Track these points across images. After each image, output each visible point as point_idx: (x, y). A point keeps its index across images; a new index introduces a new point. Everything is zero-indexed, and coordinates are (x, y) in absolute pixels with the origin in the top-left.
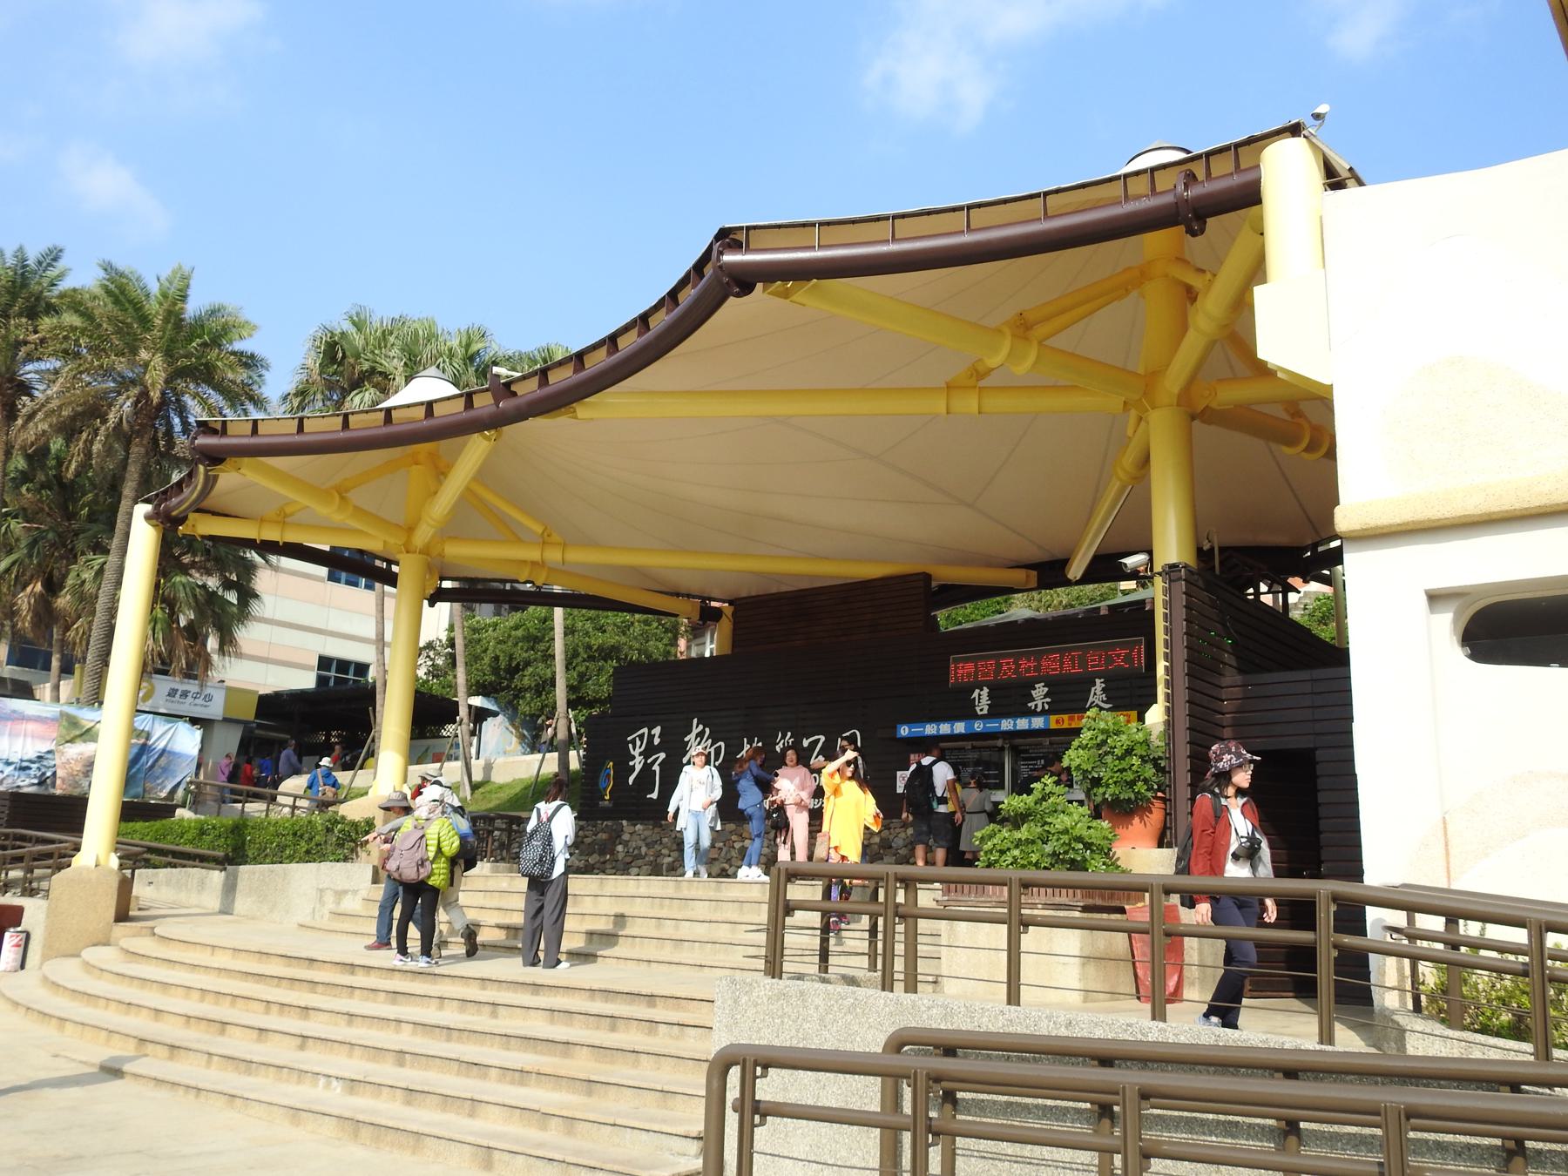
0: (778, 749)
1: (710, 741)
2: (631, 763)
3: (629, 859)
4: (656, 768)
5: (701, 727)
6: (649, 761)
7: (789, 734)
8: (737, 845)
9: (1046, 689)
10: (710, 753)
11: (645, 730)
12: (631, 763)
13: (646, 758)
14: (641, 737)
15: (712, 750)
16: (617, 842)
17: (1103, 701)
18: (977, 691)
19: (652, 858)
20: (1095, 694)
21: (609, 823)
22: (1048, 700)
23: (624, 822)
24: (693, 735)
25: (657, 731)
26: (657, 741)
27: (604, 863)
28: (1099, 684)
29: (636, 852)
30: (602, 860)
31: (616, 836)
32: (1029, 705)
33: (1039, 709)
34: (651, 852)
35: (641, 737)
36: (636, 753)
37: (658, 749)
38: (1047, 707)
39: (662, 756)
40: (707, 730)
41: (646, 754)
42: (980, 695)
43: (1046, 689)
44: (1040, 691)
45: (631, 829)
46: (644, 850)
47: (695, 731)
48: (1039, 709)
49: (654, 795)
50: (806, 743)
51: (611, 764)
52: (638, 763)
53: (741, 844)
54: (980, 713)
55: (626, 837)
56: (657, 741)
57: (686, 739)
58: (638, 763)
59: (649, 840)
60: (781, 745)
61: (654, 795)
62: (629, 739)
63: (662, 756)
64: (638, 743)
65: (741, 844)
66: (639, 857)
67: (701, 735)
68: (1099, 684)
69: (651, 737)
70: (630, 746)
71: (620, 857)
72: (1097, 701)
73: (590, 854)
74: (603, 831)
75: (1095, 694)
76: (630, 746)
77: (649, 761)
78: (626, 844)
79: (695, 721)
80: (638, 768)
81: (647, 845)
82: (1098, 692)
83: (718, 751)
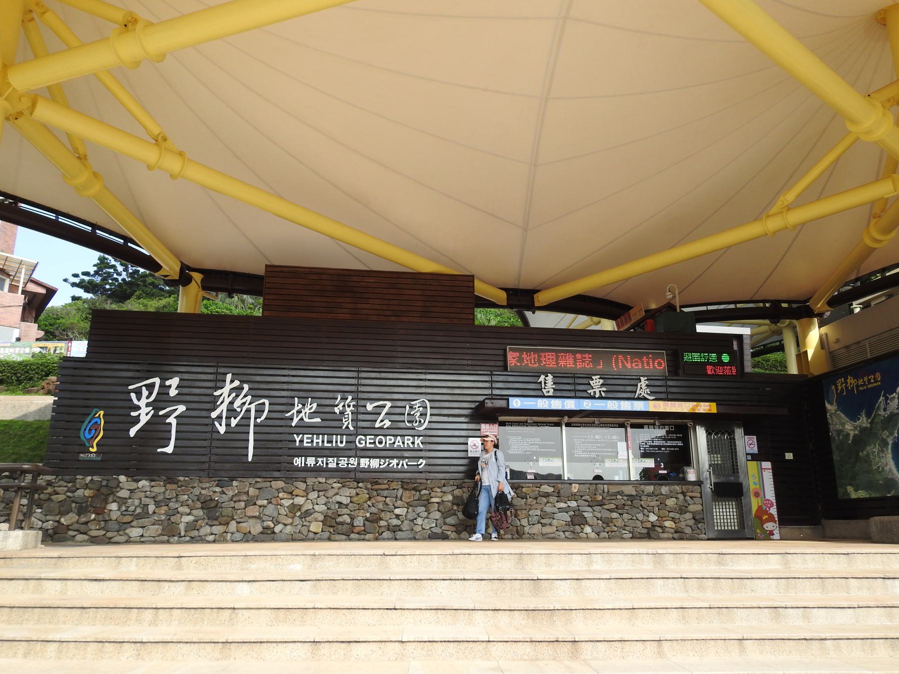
0: (337, 410)
1: (249, 398)
2: (134, 414)
3: (127, 519)
4: (172, 420)
5: (237, 383)
6: (161, 413)
7: (350, 398)
8: (287, 503)
9: (602, 381)
10: (248, 411)
11: (157, 381)
12: (134, 414)
13: (157, 409)
14: (150, 387)
15: (253, 407)
16: (111, 499)
17: (647, 394)
18: (543, 377)
19: (163, 517)
20: (641, 388)
21: (96, 478)
22: (605, 389)
23: (122, 478)
24: (226, 390)
25: (174, 382)
26: (173, 392)
27: (86, 523)
28: (643, 382)
29: (139, 510)
30: (83, 520)
31: (105, 493)
32: (589, 392)
33: (597, 395)
34: (163, 509)
35: (150, 387)
36: (142, 403)
37: (175, 401)
38: (603, 394)
39: (181, 408)
40: (246, 387)
41: (156, 405)
42: (545, 379)
43: (602, 381)
44: (596, 382)
45: (133, 485)
46: (152, 508)
47: (228, 387)
48: (597, 395)
49: (169, 449)
50: (370, 407)
51: (102, 413)
52: (145, 415)
53: (291, 501)
54: (546, 394)
55: (124, 494)
56: (173, 392)
57: (217, 393)
58: (145, 415)
59: (160, 498)
60: (340, 407)
61: (169, 449)
62: (131, 387)
63: (181, 408)
64: (145, 392)
65: (291, 501)
66: (145, 514)
67: (239, 389)
68: (643, 382)
69: (164, 388)
70: (133, 396)
71: (114, 516)
72: (643, 394)
73: (62, 514)
74: (86, 487)
75: (641, 388)
76: (133, 396)
77: (161, 413)
78: (122, 501)
79: (229, 377)
80: (144, 419)
81: (158, 504)
82: (644, 387)
83: (259, 411)
